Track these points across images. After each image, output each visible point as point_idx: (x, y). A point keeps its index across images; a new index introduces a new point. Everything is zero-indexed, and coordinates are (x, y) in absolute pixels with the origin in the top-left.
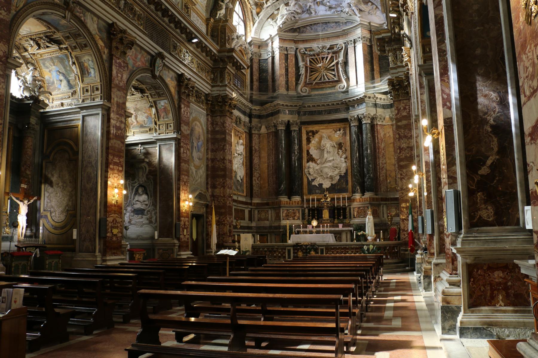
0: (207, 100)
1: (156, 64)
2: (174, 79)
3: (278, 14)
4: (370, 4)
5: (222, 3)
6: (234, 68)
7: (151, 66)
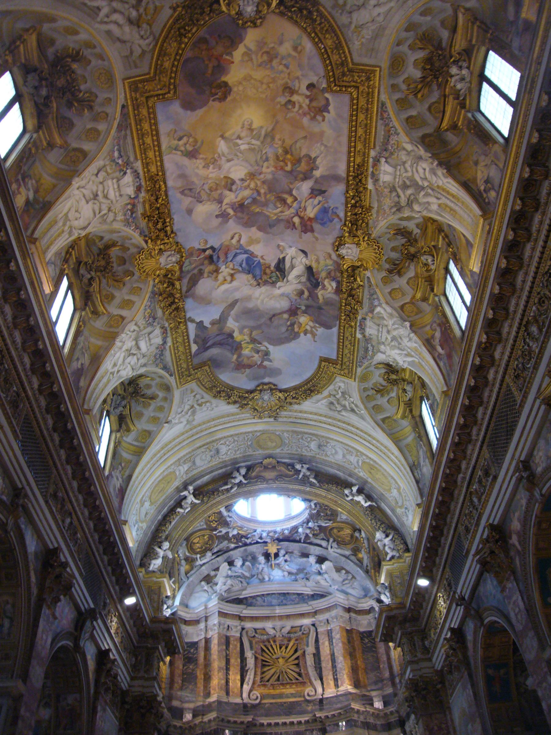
0: (124, 702)
1: (85, 628)
2: (94, 657)
3: (216, 576)
4: (344, 572)
5: (159, 550)
6: (166, 650)
7: (76, 629)
